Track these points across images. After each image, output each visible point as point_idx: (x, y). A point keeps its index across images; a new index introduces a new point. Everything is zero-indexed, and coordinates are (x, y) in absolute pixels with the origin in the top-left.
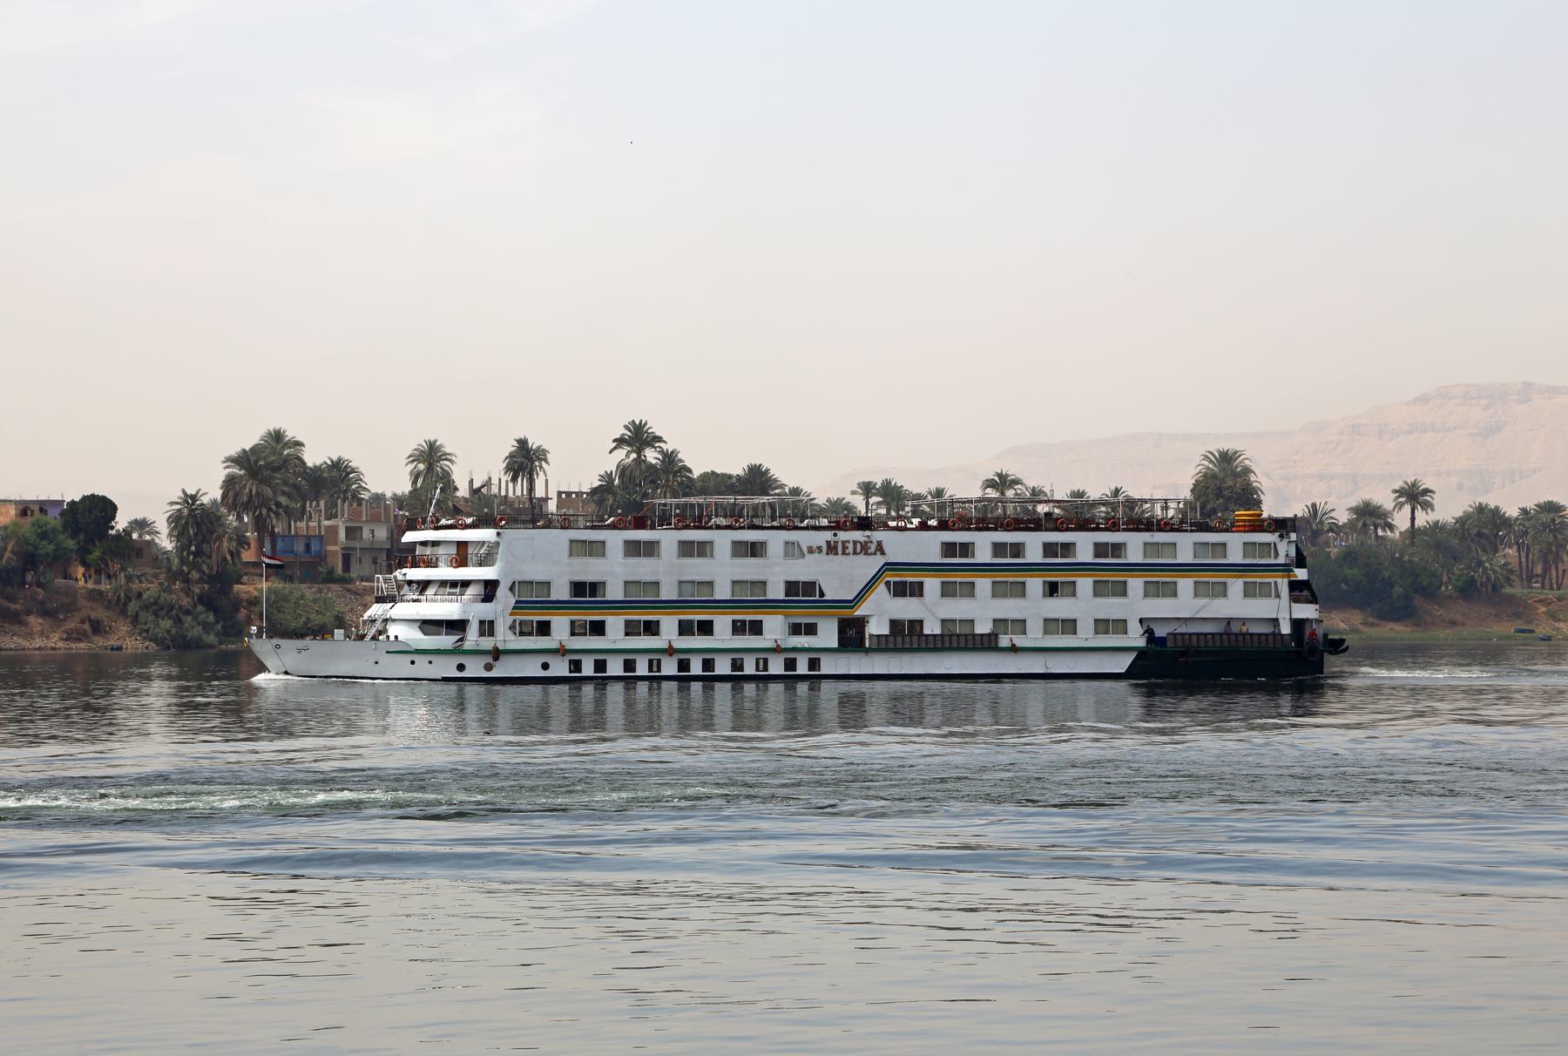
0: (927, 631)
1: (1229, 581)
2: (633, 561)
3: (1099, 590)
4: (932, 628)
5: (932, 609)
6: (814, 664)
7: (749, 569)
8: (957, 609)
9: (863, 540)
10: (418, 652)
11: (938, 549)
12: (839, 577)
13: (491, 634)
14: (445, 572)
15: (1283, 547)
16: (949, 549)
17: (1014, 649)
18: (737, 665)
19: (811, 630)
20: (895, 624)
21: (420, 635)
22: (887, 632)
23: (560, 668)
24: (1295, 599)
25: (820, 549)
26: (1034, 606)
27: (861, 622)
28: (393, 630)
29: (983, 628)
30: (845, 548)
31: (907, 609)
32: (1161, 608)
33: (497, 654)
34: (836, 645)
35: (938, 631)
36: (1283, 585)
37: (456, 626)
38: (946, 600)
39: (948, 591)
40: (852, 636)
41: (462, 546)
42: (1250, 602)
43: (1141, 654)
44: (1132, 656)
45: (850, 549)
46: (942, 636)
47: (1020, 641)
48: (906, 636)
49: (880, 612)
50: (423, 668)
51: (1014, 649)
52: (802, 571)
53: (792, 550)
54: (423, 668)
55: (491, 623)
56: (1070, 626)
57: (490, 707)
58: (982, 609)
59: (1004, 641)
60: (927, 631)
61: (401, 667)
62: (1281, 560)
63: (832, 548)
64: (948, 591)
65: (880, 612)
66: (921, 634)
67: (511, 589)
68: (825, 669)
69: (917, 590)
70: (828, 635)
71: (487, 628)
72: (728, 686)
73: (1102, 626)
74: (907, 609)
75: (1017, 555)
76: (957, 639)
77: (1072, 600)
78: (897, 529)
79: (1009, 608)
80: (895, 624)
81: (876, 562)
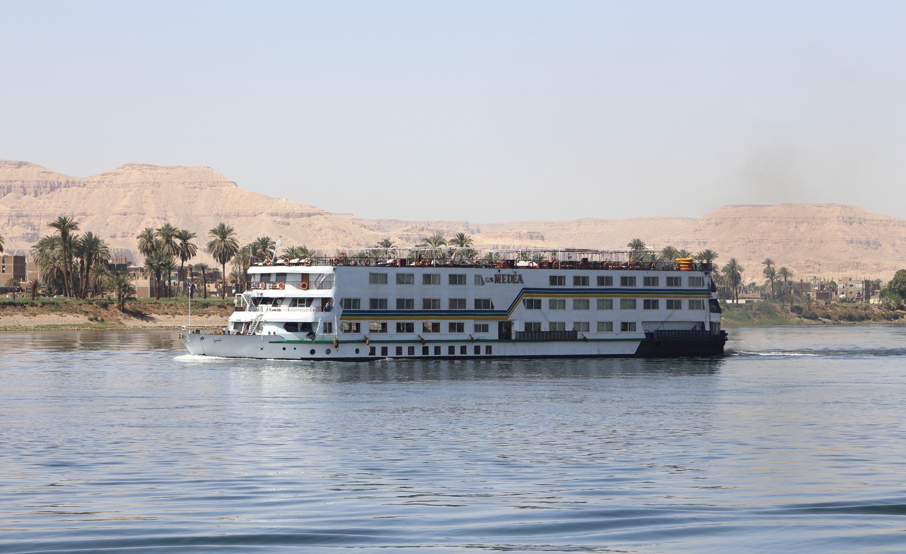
0: (543, 330)
1: (682, 300)
2: (374, 286)
3: (462, 302)
4: (545, 328)
5: (545, 317)
6: (489, 349)
7: (457, 292)
8: (557, 316)
9: (512, 274)
10: (289, 342)
11: (547, 280)
12: (502, 296)
13: (330, 331)
14: (291, 291)
15: (707, 280)
16: (553, 280)
17: (585, 340)
18: (451, 350)
19: (485, 329)
20: (528, 325)
21: (285, 332)
22: (523, 330)
23: (365, 352)
24: (712, 311)
25: (491, 279)
26: (594, 315)
27: (509, 325)
28: (267, 330)
29: (569, 328)
30: (504, 279)
31: (533, 316)
32: (652, 315)
33: (338, 343)
34: (497, 338)
35: (548, 330)
36: (706, 301)
37: (307, 327)
38: (552, 311)
39: (552, 306)
40: (505, 335)
41: (305, 276)
42: (692, 312)
43: (643, 342)
44: (638, 344)
45: (506, 280)
46: (550, 332)
47: (588, 336)
48: (532, 333)
49: (520, 319)
50: (290, 352)
51: (585, 340)
52: (484, 292)
53: (479, 281)
54: (290, 352)
55: (330, 324)
56: (609, 326)
57: (437, 369)
58: (568, 317)
59: (579, 336)
60: (543, 330)
61: (277, 351)
62: (706, 287)
63: (497, 279)
64: (552, 306)
65: (520, 319)
66: (539, 331)
67: (341, 303)
68: (495, 353)
69: (538, 305)
70: (493, 332)
71: (328, 328)
72: (447, 362)
73: (625, 327)
74: (533, 316)
75: (560, 284)
76: (558, 334)
77: (609, 311)
78: (316, 260)
79: (581, 316)
80: (528, 325)
81: (518, 288)
